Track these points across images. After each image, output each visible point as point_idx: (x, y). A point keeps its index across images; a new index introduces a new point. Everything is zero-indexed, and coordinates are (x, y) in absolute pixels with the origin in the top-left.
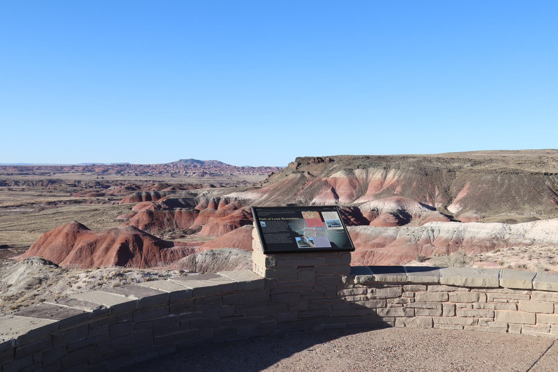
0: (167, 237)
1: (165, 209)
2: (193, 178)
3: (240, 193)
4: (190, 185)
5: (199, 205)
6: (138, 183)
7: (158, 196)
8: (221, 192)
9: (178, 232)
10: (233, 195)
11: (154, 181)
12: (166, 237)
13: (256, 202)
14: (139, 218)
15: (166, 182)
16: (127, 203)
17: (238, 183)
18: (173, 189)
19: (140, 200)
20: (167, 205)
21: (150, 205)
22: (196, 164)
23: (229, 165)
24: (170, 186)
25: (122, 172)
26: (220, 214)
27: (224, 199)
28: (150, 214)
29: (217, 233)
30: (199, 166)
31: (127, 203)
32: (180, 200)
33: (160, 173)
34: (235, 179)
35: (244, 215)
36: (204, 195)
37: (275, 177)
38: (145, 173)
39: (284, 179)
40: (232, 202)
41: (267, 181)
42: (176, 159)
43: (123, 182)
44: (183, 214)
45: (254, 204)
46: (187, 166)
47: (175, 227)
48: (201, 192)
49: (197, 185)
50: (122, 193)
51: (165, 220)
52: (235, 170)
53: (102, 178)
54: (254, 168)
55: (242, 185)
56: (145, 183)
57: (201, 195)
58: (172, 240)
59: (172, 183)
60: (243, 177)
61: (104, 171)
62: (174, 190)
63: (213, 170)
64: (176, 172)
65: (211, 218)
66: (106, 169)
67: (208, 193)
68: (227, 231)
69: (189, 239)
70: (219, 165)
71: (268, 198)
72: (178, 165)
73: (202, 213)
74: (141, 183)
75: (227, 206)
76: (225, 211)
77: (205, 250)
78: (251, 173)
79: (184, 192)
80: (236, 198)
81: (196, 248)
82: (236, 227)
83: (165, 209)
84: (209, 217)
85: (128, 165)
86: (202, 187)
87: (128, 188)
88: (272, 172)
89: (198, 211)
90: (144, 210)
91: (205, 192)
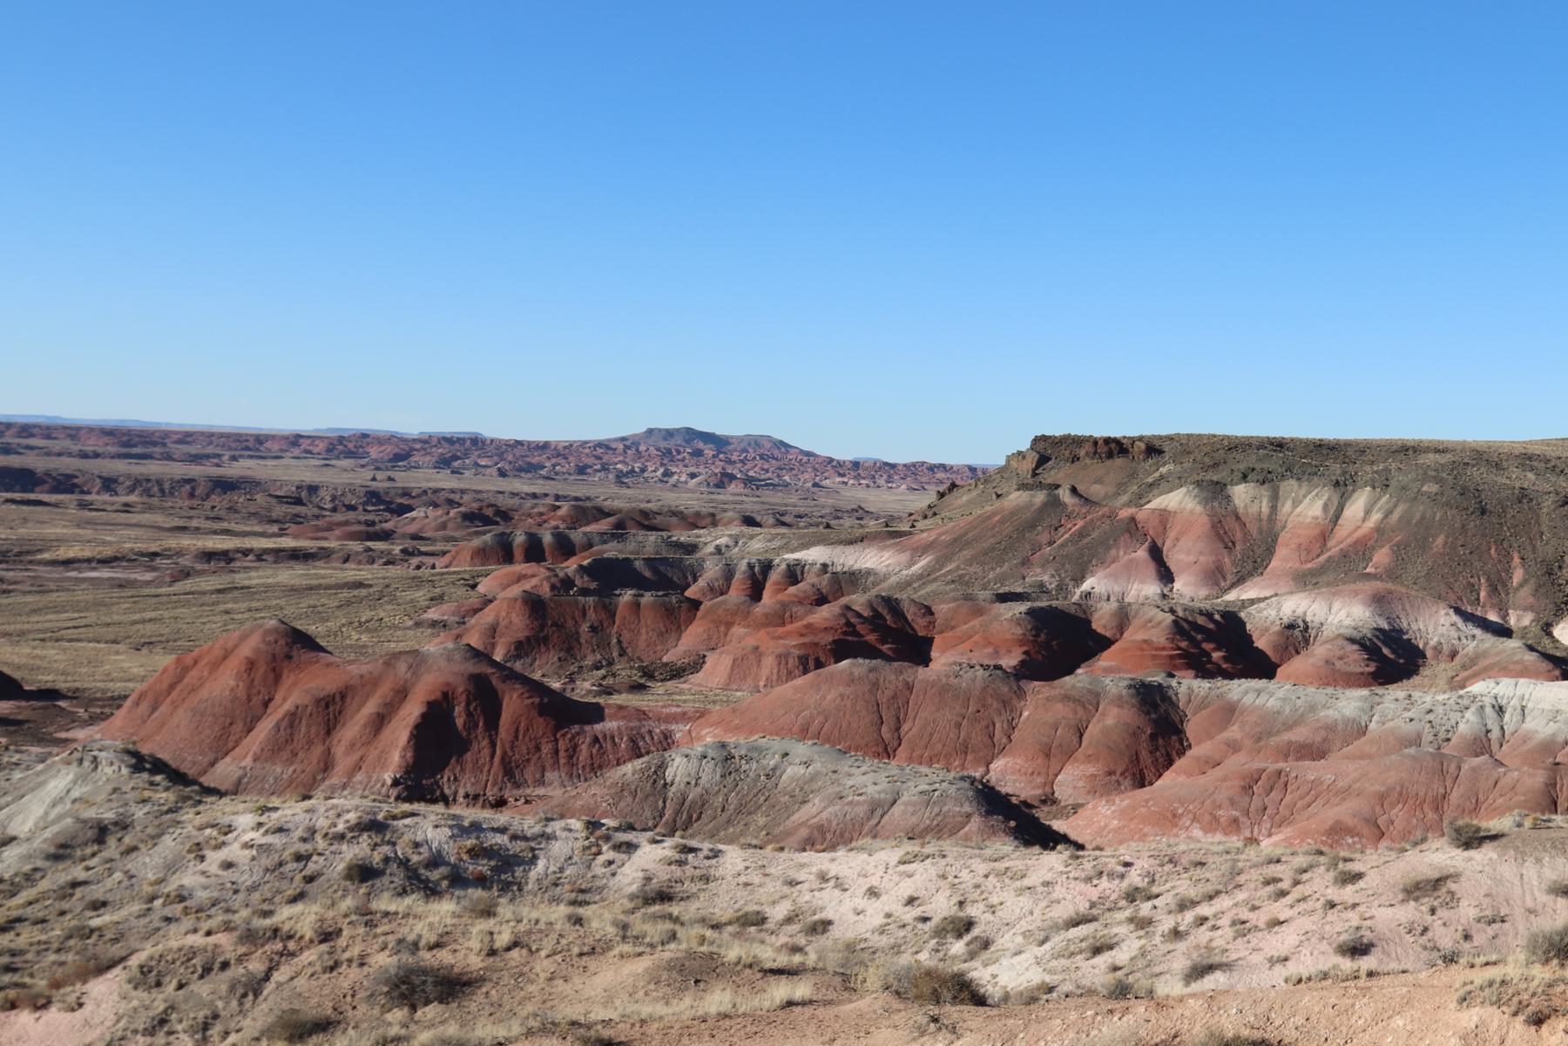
0: (587, 685)
1: (585, 592)
2: (687, 493)
3: (839, 549)
4: (674, 514)
5: (701, 583)
6: (505, 502)
7: (565, 548)
8: (776, 543)
9: (625, 672)
10: (815, 555)
11: (557, 498)
12: (584, 689)
13: (893, 580)
14: (497, 617)
15: (599, 502)
16: (464, 567)
17: (838, 513)
18: (620, 525)
19: (507, 556)
20: (593, 577)
21: (537, 578)
22: (701, 445)
23: (809, 454)
24: (609, 515)
25: (456, 464)
26: (766, 615)
27: (784, 566)
28: (534, 604)
29: (756, 679)
30: (709, 452)
31: (464, 567)
32: (638, 565)
33: (581, 470)
34: (827, 501)
35: (848, 624)
36: (718, 550)
37: (961, 499)
38: (531, 468)
39: (988, 508)
40: (811, 578)
41: (931, 512)
42: (633, 426)
43: (456, 497)
44: (644, 612)
45: (883, 589)
46: (669, 451)
47: (615, 654)
48: (711, 539)
49: (698, 514)
50: (448, 533)
51: (585, 627)
52: (830, 472)
53: (390, 479)
54: (893, 466)
55: (848, 522)
56: (529, 503)
57: (710, 549)
58: (601, 700)
59: (617, 504)
60: (855, 493)
61: (398, 457)
62: (620, 530)
63: (759, 472)
64: (633, 471)
65: (738, 630)
66: (403, 451)
67: (731, 543)
68: (790, 676)
69: (657, 698)
70: (776, 452)
71: (934, 570)
72: (642, 448)
73: (708, 612)
74: (516, 501)
75: (792, 590)
76: (784, 606)
77: (709, 737)
78: (881, 482)
79: (653, 537)
80: (825, 566)
81: (679, 731)
82: (819, 665)
83: (585, 592)
84: (729, 625)
85: (477, 442)
86: (715, 524)
87: (469, 517)
88: (948, 482)
89: (695, 605)
90: (516, 591)
91: (723, 541)
